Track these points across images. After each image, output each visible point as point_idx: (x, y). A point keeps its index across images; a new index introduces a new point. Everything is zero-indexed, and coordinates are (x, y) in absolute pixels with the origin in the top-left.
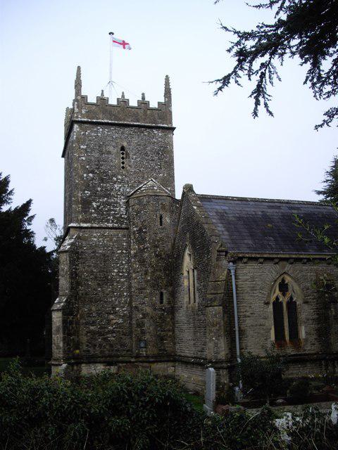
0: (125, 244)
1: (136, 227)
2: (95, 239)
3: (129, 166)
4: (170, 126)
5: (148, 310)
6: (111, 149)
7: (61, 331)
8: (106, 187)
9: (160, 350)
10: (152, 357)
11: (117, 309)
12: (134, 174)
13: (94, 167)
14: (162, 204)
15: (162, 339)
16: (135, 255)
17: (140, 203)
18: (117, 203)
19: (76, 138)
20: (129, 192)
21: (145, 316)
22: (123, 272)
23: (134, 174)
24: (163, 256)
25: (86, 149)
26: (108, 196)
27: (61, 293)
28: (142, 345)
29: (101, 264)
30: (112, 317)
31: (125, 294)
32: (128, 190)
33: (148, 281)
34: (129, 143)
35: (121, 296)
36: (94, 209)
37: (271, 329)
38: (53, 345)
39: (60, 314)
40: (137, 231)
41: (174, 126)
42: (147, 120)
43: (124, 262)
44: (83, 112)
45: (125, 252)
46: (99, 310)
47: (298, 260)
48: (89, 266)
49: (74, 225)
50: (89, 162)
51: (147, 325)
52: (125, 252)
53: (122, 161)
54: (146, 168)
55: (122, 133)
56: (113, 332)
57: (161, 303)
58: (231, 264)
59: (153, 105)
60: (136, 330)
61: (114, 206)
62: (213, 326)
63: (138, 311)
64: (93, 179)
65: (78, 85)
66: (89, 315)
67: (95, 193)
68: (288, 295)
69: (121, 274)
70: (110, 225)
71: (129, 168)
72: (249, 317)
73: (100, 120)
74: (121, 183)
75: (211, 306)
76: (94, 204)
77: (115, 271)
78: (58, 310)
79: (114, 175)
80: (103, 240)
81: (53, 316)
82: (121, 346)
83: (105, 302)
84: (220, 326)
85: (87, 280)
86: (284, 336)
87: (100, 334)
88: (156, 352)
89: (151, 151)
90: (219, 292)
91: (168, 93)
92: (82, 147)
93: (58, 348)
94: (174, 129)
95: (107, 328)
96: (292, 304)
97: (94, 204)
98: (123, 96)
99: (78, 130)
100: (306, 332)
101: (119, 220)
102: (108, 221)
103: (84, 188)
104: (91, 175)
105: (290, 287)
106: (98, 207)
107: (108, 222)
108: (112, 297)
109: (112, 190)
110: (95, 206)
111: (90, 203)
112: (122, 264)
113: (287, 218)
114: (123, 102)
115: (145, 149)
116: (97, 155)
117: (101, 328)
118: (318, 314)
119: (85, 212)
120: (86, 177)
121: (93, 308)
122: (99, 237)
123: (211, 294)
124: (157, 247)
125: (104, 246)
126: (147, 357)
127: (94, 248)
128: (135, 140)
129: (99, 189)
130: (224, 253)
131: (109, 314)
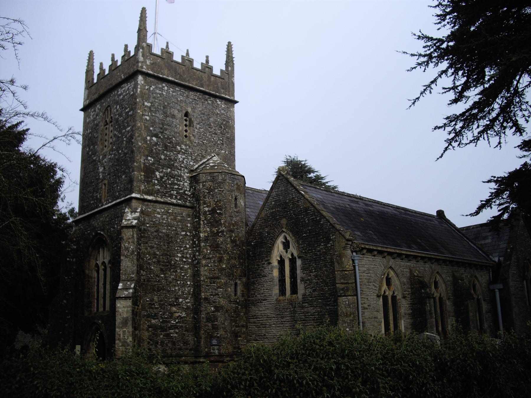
0: (189, 225)
1: (207, 207)
2: (159, 216)
3: (193, 135)
4: (232, 98)
5: (223, 302)
6: (176, 112)
7: (130, 323)
8: (170, 156)
9: (235, 348)
10: (227, 356)
11: (181, 300)
12: (198, 145)
13: (158, 130)
14: (237, 184)
15: (236, 335)
16: (206, 239)
17: (213, 180)
18: (180, 176)
19: (140, 91)
20: (193, 166)
21: (217, 309)
22: (186, 258)
23: (198, 145)
24: (238, 243)
25: (150, 108)
26: (172, 167)
27: (123, 277)
28: (214, 342)
29: (164, 245)
30: (174, 309)
31: (189, 283)
32: (191, 163)
33: (224, 269)
34: (193, 109)
35: (184, 285)
36: (157, 180)
37: (382, 322)
38: (117, 342)
39: (129, 303)
40: (209, 211)
41: (236, 99)
42: (211, 87)
43: (188, 246)
44: (148, 62)
45: (188, 234)
46: (161, 301)
47: (399, 255)
48: (152, 247)
49: (138, 196)
50: (153, 123)
51: (221, 319)
52: (188, 234)
53: (185, 128)
54: (209, 141)
55: (187, 97)
56: (175, 327)
57: (235, 295)
58: (354, 254)
59: (217, 72)
60: (205, 326)
61: (177, 180)
62: (347, 316)
63: (209, 303)
64: (156, 144)
65: (142, 31)
66: (151, 305)
67: (158, 161)
68: (393, 288)
69: (184, 260)
70: (174, 201)
71: (192, 138)
72: (367, 309)
73: (165, 77)
74: (184, 154)
75: (344, 296)
76: (157, 173)
77: (179, 255)
78: (126, 298)
79: (178, 144)
80: (167, 218)
81: (118, 305)
82: (184, 343)
83: (169, 291)
84: (354, 317)
85: (149, 264)
86: (389, 329)
87: (163, 329)
88: (231, 350)
89: (214, 123)
90: (350, 282)
91: (230, 61)
92: (146, 104)
93: (125, 344)
94: (236, 102)
95: (169, 322)
96: (394, 298)
97: (157, 173)
98: (188, 54)
99: (143, 82)
100: (405, 327)
101: (183, 196)
102: (171, 196)
103: (146, 153)
104: (154, 139)
105: (393, 281)
106: (162, 178)
107: (172, 198)
108: (175, 286)
109: (176, 160)
110: (158, 177)
111: (153, 173)
112: (186, 248)
113: (370, 214)
114: (187, 61)
115: (208, 119)
116: (161, 117)
117: (163, 322)
118: (412, 309)
119: (148, 182)
120: (150, 140)
121: (156, 298)
122: (163, 214)
123: (342, 283)
124: (232, 231)
125: (168, 225)
126: (221, 355)
127: (157, 225)
128: (200, 107)
129: (163, 157)
130: (351, 243)
131: (172, 305)
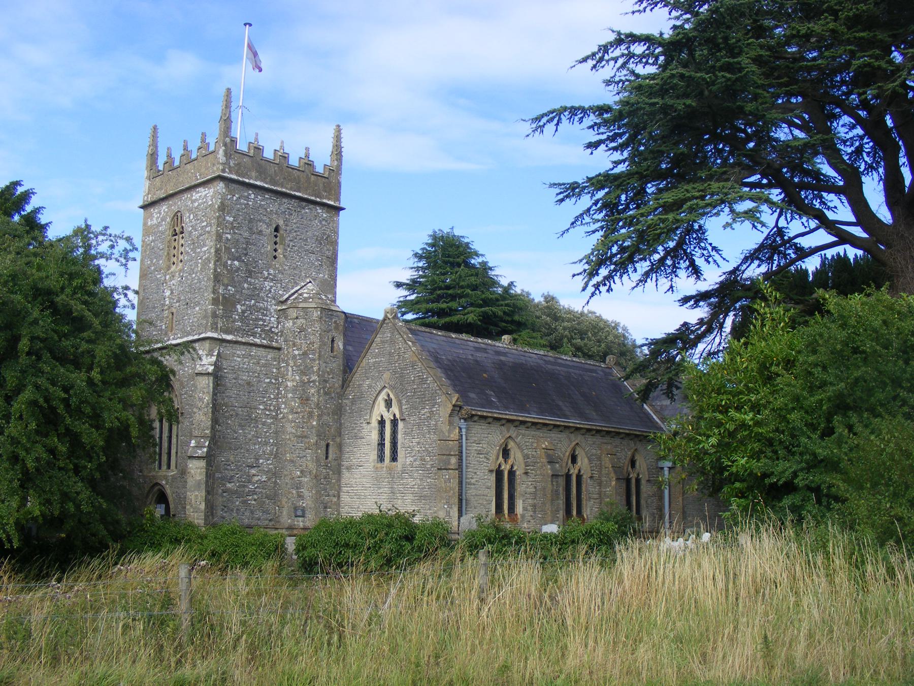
0: (275, 370)
1: (297, 349)
4: (336, 204)
7: (203, 486)
11: (261, 461)
18: (266, 309)
20: (282, 296)
22: (270, 410)
24: (333, 395)
29: (245, 395)
30: (253, 471)
32: (280, 292)
35: (266, 443)
38: (188, 507)
39: (202, 464)
40: (299, 355)
41: (342, 205)
43: (272, 396)
45: (273, 381)
52: (273, 381)
58: (462, 421)
59: (319, 169)
64: (238, 269)
68: (510, 462)
69: (267, 413)
70: (258, 341)
72: (474, 484)
73: (252, 181)
74: (272, 280)
77: (261, 407)
83: (248, 450)
84: (454, 493)
92: (227, 218)
93: (197, 510)
94: (343, 209)
97: (239, 307)
104: (236, 263)
106: (243, 312)
109: (262, 289)
110: (240, 311)
116: (246, 234)
120: (231, 265)
122: (244, 356)
129: (246, 286)
